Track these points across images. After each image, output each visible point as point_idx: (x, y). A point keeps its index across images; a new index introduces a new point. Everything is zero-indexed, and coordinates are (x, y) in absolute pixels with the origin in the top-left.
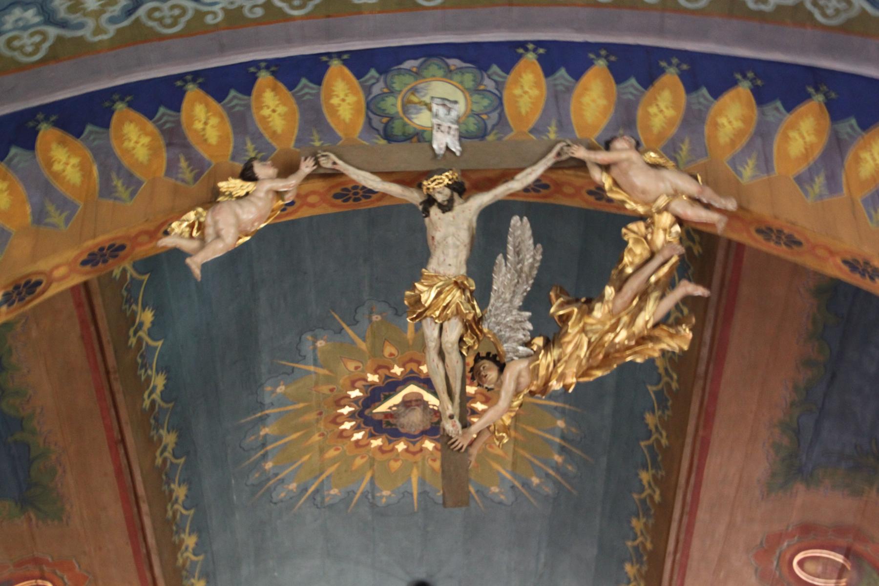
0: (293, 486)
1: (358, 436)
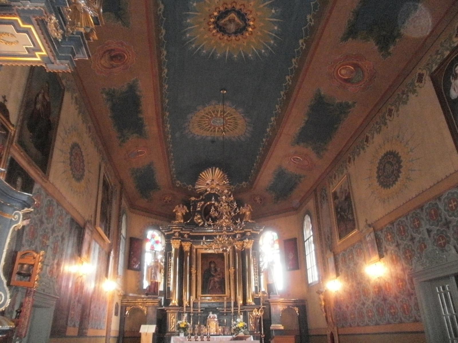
0: (194, 46)
1: (214, 31)
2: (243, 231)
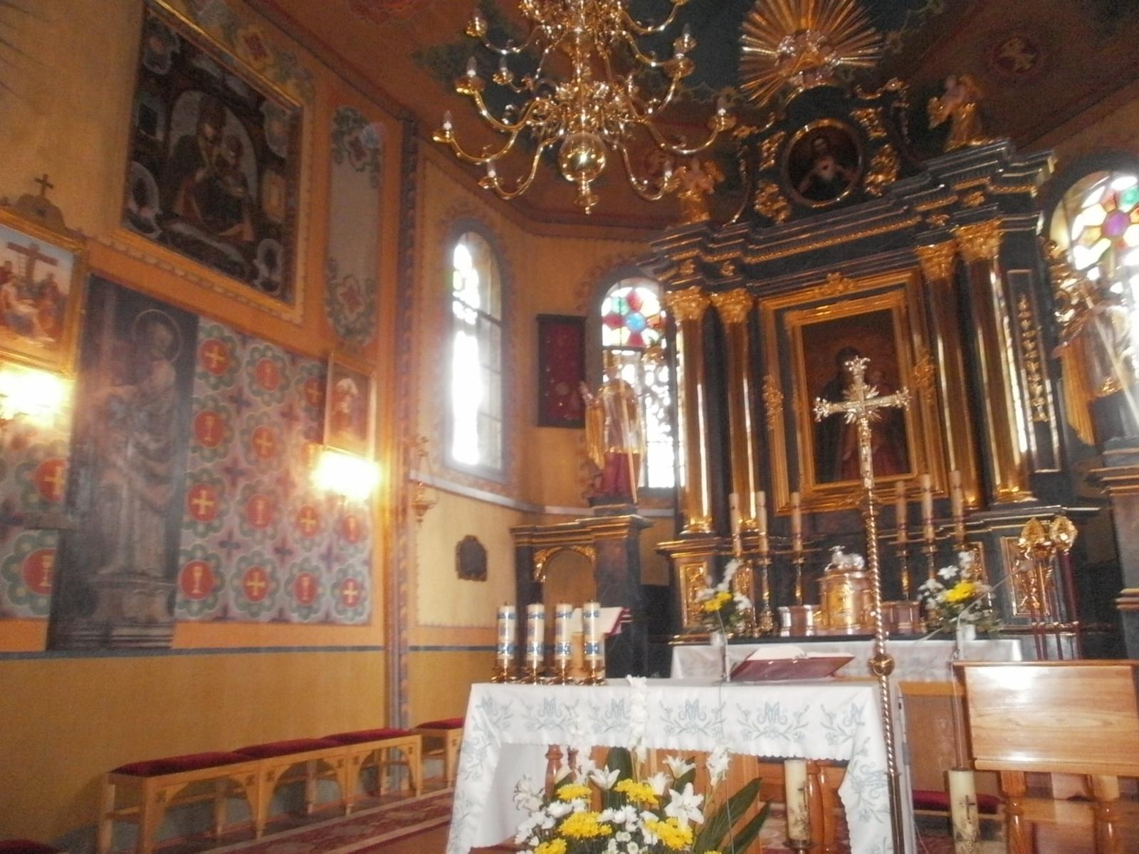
2: (954, 198)
